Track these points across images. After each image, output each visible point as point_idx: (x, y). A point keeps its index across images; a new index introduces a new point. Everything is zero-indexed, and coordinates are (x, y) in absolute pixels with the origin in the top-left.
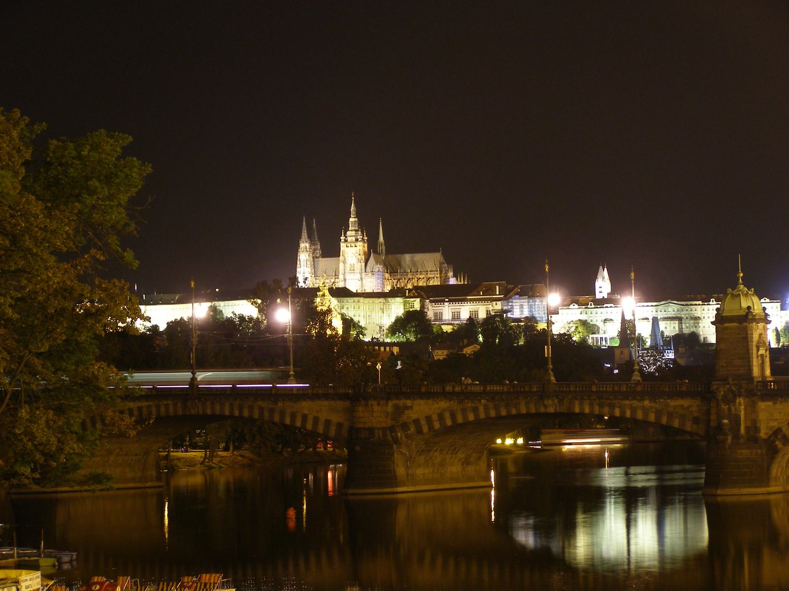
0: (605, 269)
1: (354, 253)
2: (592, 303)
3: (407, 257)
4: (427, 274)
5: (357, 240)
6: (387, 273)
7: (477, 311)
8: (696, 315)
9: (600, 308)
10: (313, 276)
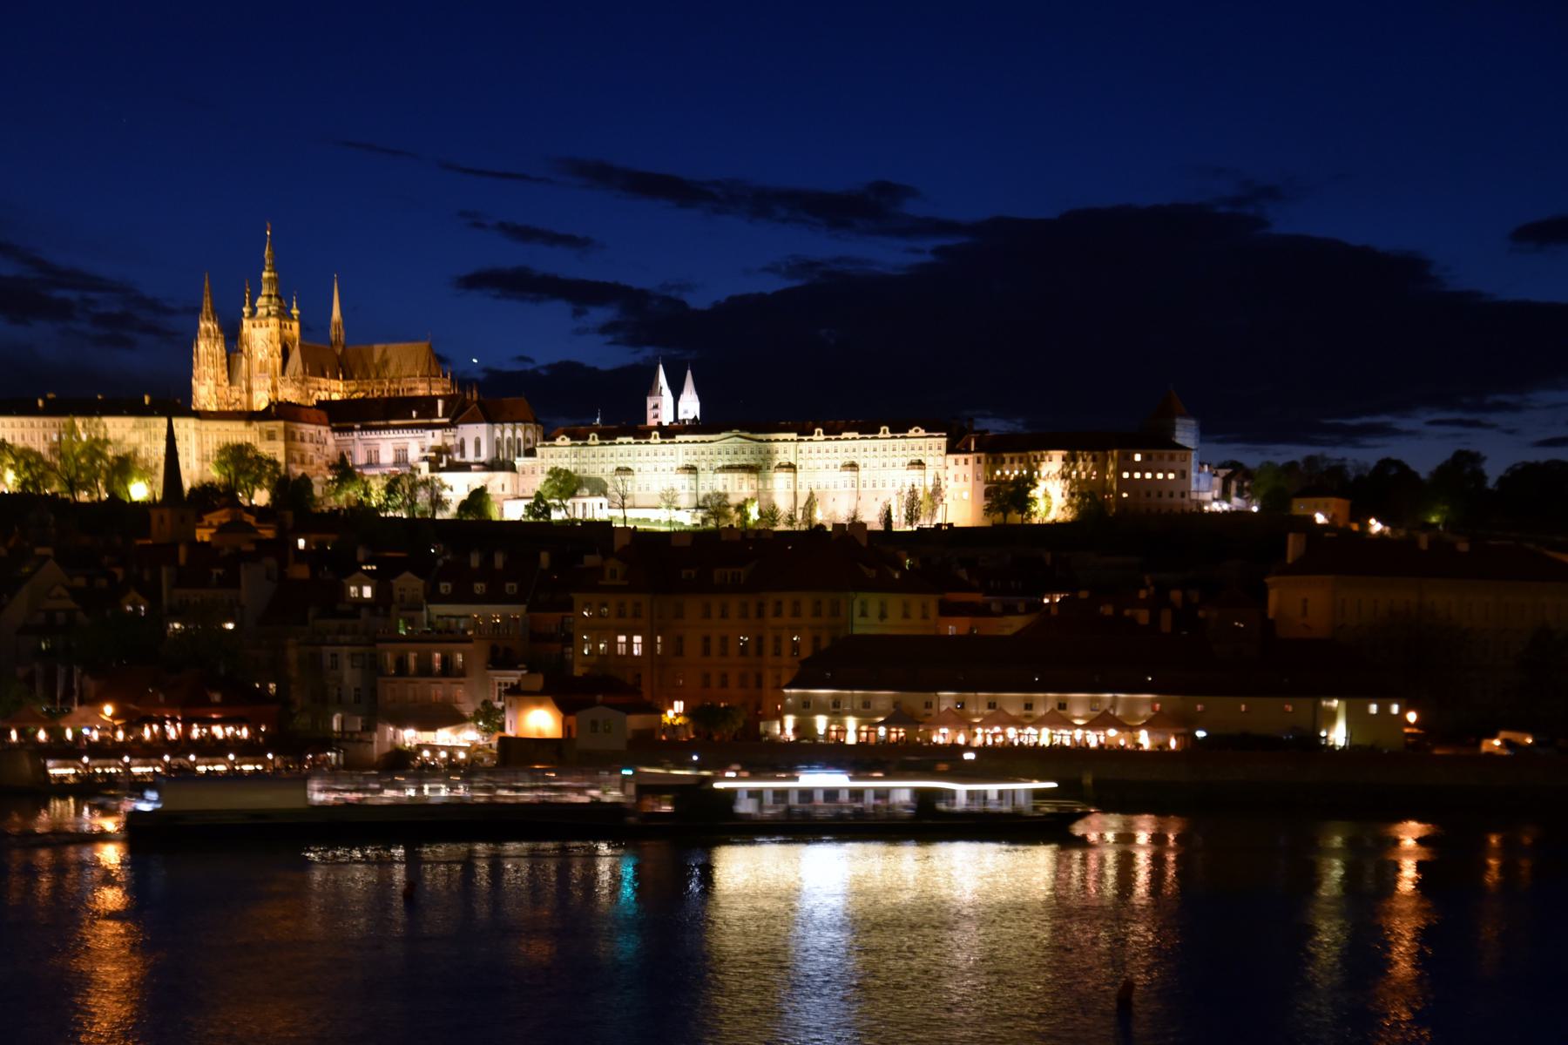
0: (689, 373)
1: (265, 340)
2: (596, 436)
3: (378, 349)
4: (399, 383)
5: (269, 314)
6: (339, 379)
7: (406, 450)
8: (785, 462)
9: (610, 444)
10: (227, 384)
